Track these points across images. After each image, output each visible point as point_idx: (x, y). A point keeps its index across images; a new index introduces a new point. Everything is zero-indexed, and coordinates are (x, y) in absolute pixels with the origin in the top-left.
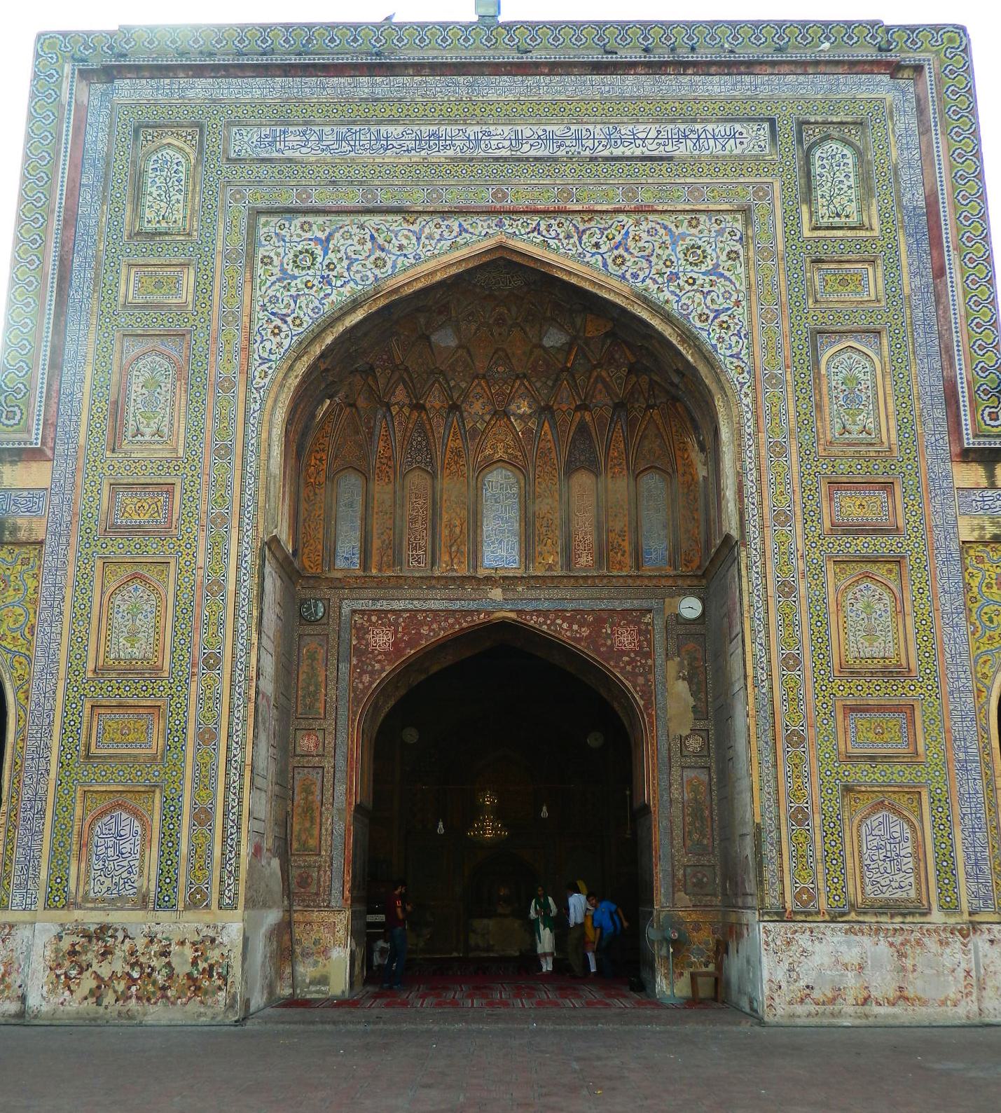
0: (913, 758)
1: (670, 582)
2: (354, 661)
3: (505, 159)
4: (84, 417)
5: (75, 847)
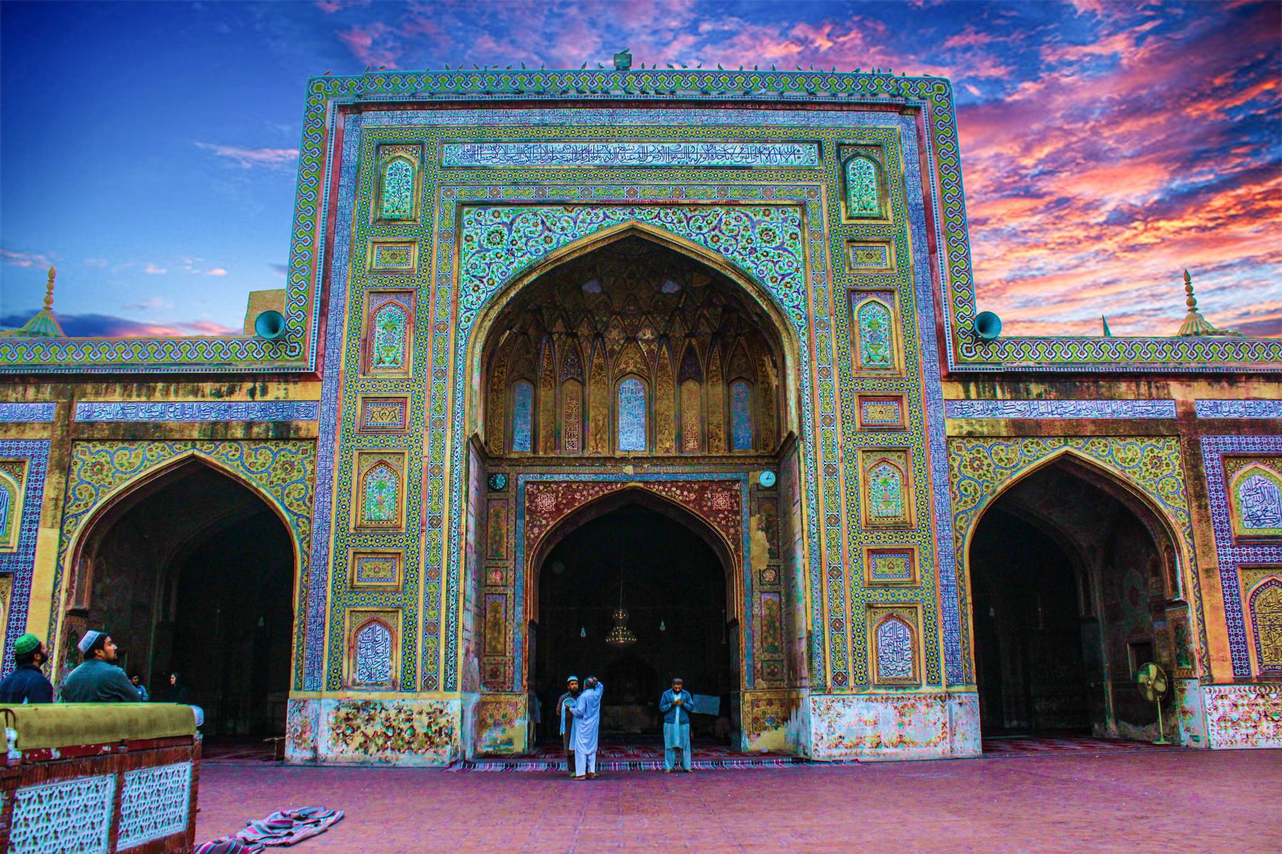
0: (913, 585)
1: (753, 461)
2: (527, 518)
3: (636, 167)
4: (344, 350)
5: (346, 649)
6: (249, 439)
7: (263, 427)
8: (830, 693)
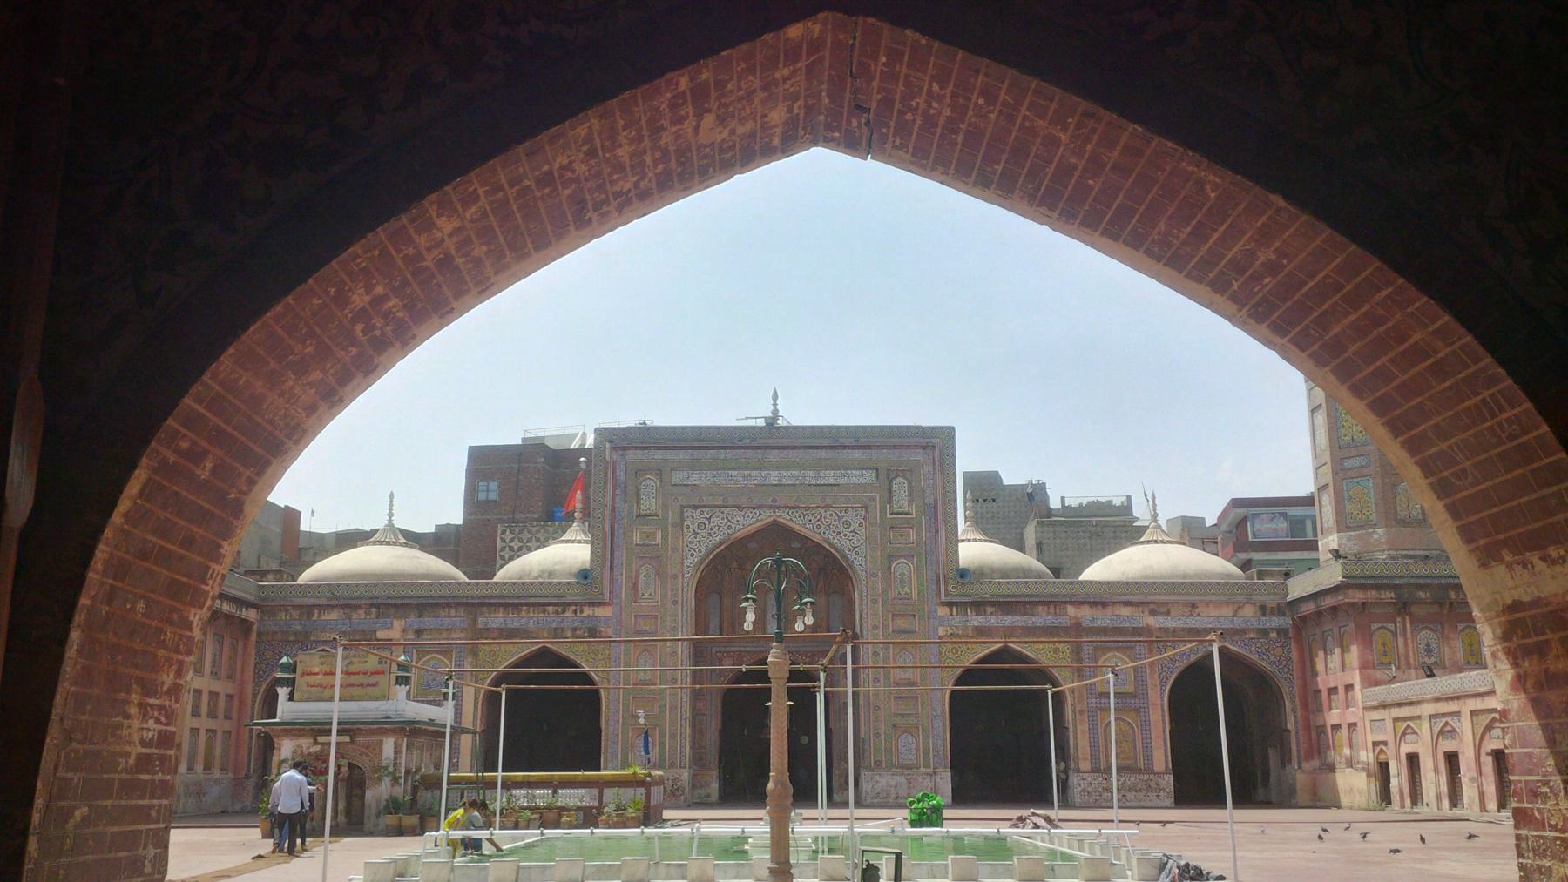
3: (776, 485)
8: (873, 771)
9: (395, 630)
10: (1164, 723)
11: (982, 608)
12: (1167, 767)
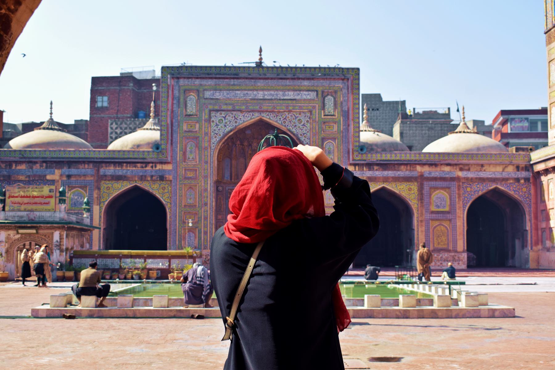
6: (152, 180)
7: (156, 177)
9: (56, 175)
10: (464, 226)
11: (372, 167)
12: (464, 249)
